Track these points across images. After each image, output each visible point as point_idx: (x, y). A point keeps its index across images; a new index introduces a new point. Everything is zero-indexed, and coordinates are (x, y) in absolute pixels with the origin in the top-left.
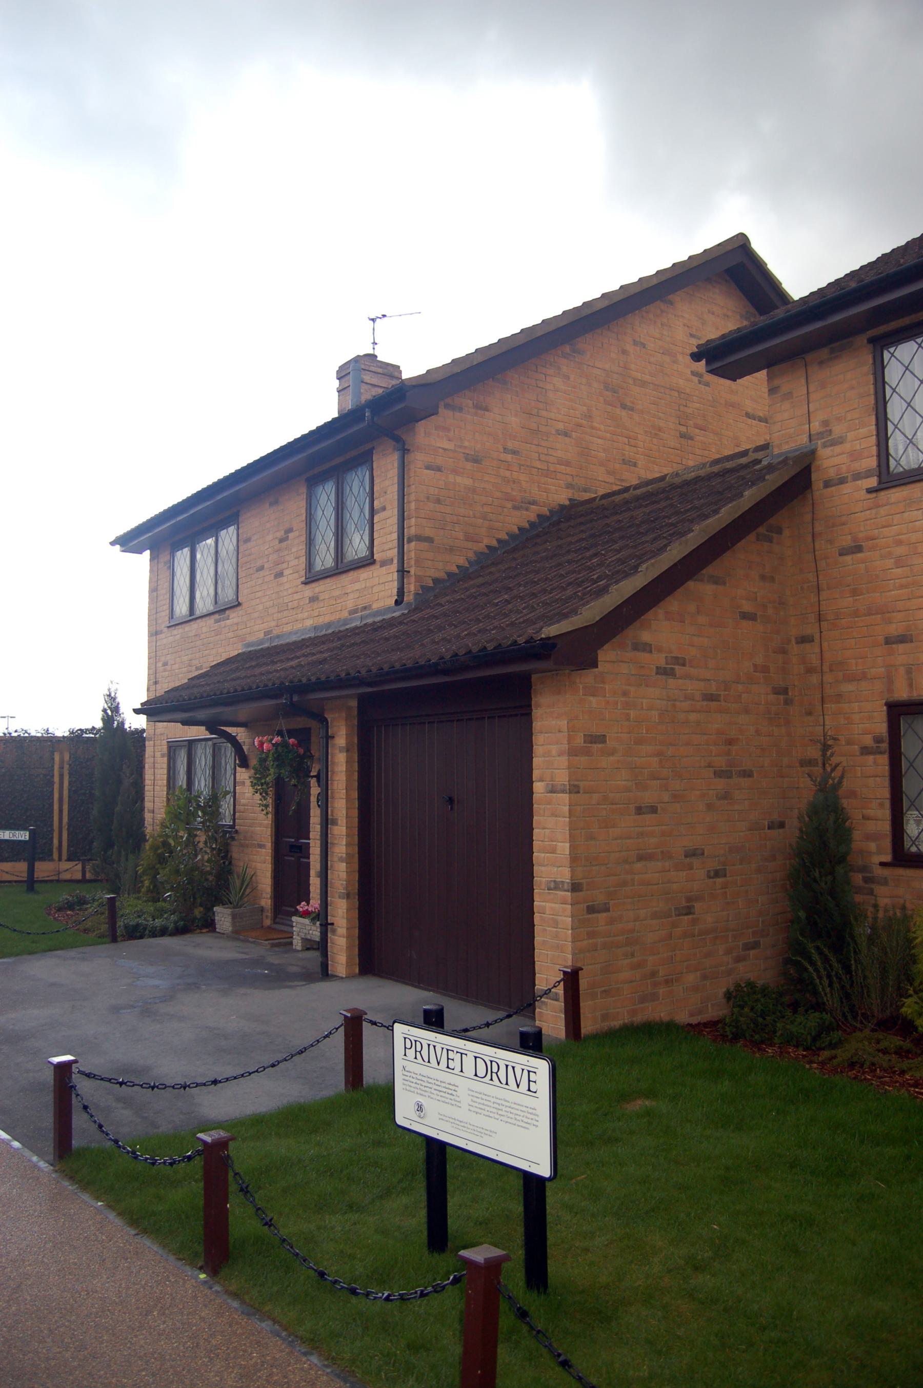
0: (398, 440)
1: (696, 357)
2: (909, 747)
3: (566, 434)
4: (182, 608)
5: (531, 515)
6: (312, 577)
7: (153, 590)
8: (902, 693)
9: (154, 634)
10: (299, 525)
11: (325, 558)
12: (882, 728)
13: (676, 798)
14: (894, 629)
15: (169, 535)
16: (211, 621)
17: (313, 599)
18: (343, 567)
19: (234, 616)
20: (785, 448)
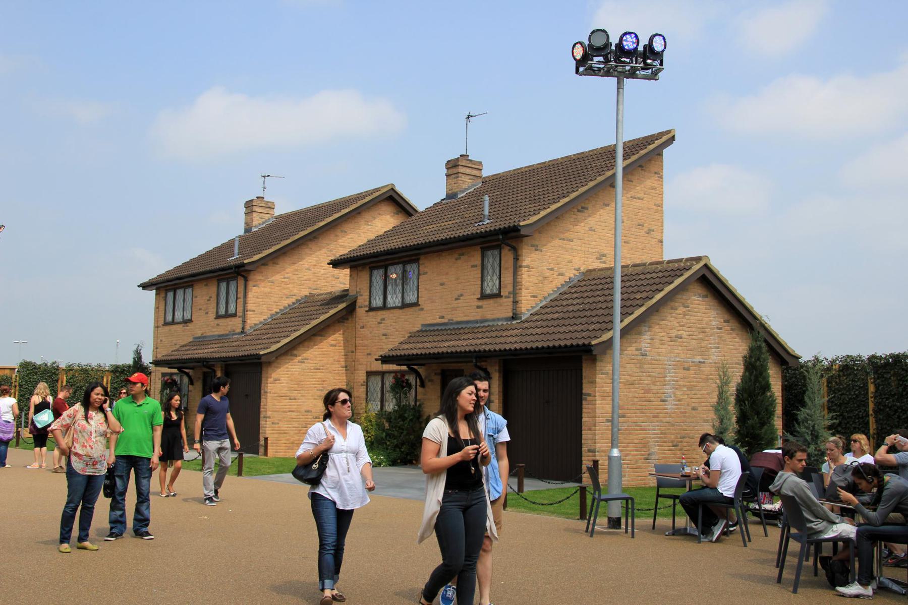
0: (243, 276)
1: (329, 264)
2: (370, 384)
3: (309, 269)
4: (169, 318)
5: (293, 300)
6: (218, 317)
7: (157, 308)
8: (369, 370)
9: (156, 327)
10: (214, 296)
11: (222, 311)
12: (365, 378)
13: (303, 396)
14: (368, 351)
15: (167, 286)
16: (181, 326)
17: (218, 325)
18: (227, 315)
19: (190, 326)
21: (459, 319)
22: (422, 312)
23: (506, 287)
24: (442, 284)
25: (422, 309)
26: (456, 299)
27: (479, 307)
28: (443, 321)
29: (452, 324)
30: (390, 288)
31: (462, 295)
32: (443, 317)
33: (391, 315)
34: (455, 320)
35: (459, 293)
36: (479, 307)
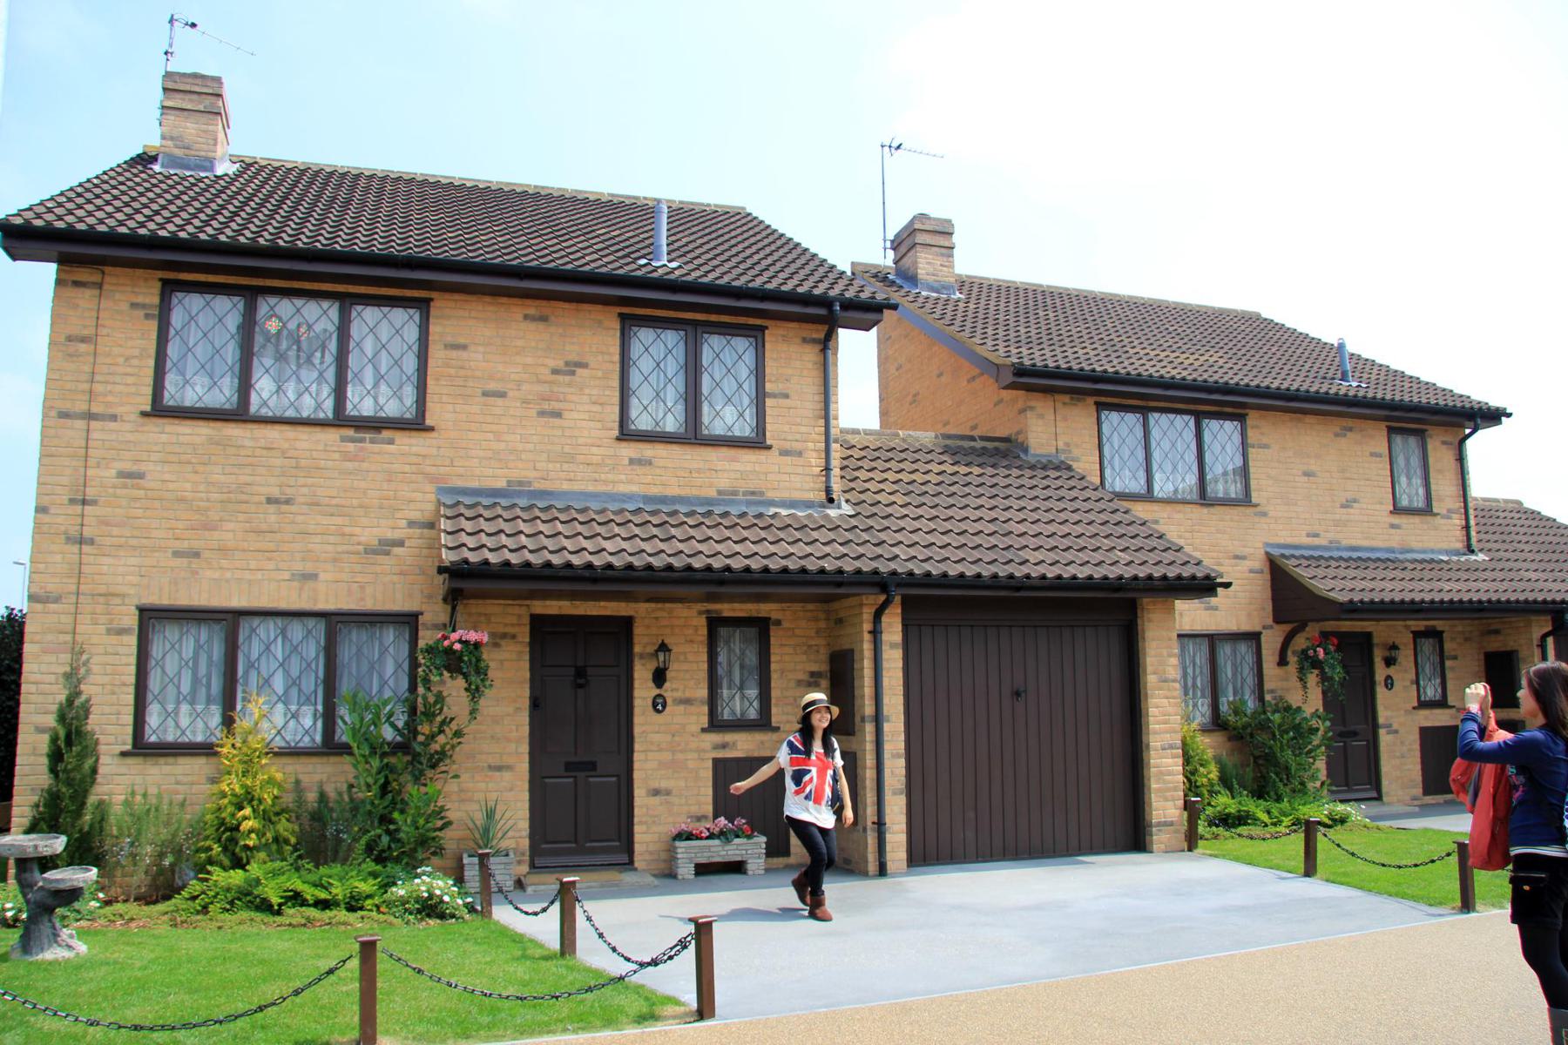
20: (1039, 452)
21: (1354, 543)
22: (1263, 520)
23: (1440, 500)
24: (1307, 474)
25: (1264, 514)
26: (1343, 506)
27: (1393, 526)
28: (1316, 541)
29: (1338, 549)
30: (1156, 455)
31: (1355, 501)
32: (1317, 535)
33: (1180, 516)
34: (1345, 543)
35: (1350, 495)
36: (1393, 526)
